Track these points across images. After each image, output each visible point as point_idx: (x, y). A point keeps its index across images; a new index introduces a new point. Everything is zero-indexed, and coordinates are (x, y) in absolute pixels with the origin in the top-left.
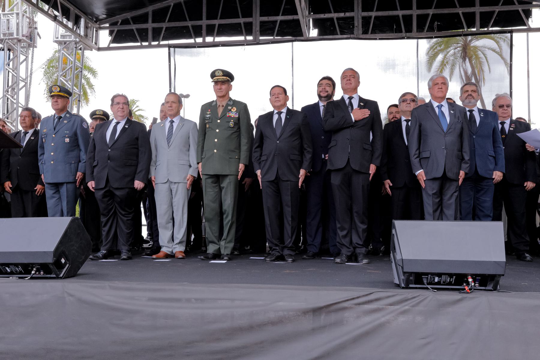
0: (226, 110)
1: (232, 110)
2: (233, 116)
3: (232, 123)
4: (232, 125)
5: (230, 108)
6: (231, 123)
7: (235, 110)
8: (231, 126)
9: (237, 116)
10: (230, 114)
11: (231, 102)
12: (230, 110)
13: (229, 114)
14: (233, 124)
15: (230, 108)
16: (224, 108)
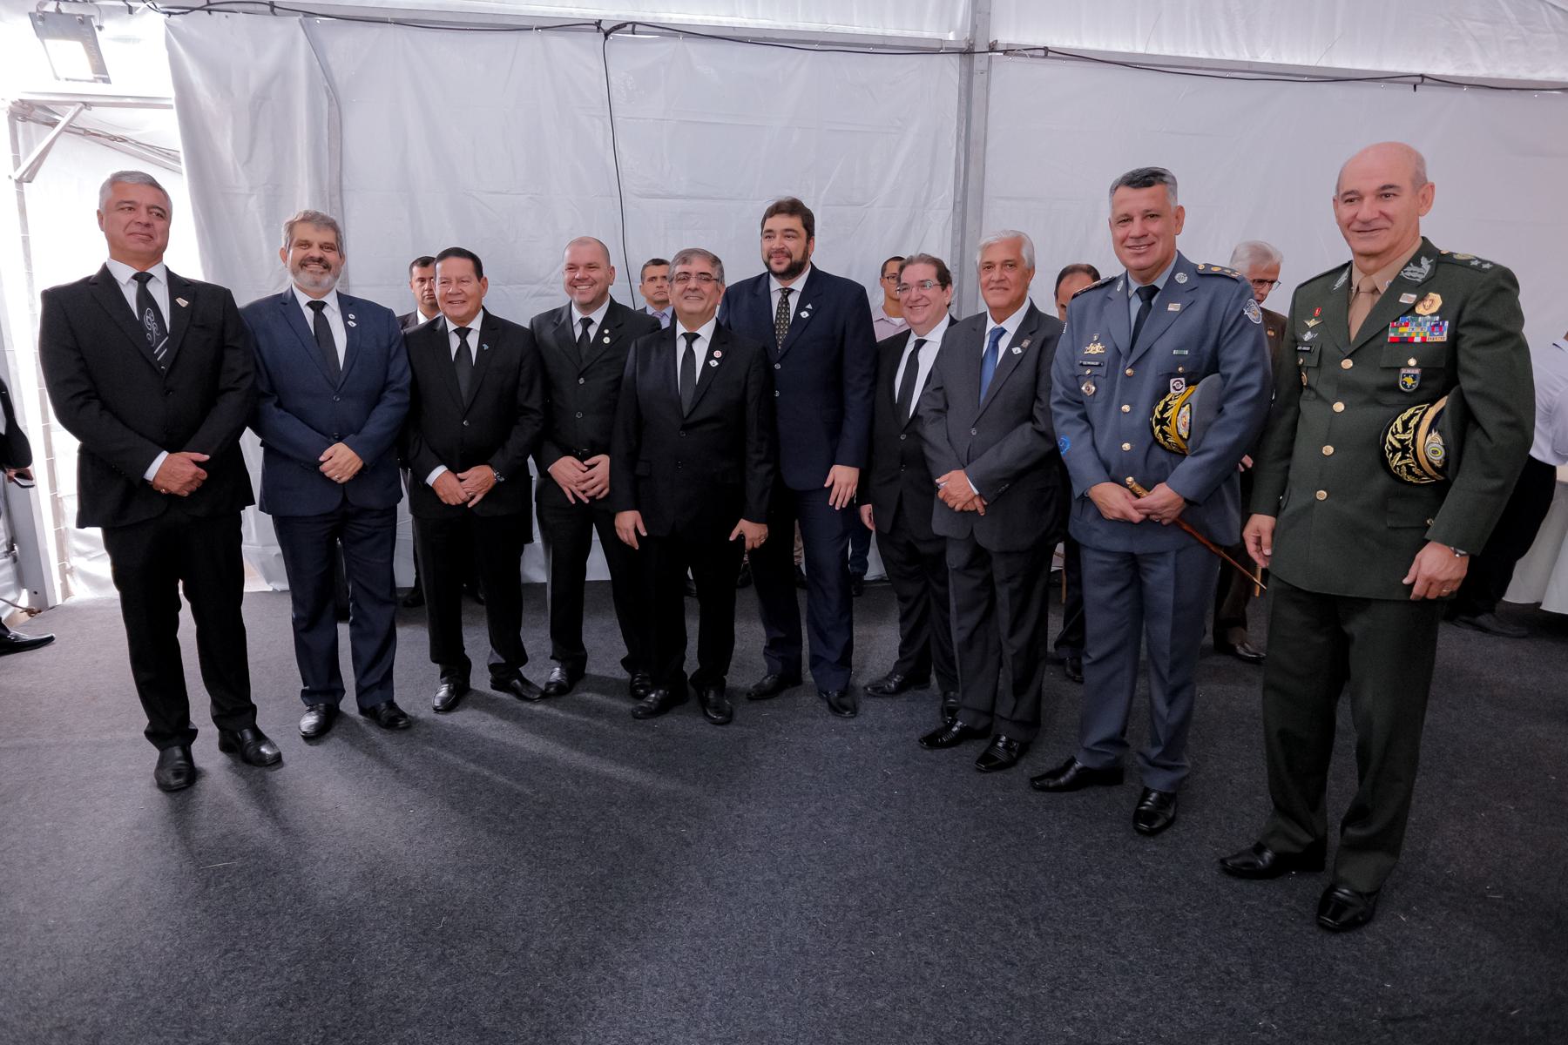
0: (1390, 308)
1: (1419, 310)
2: (1418, 340)
3: (1409, 371)
4: (1409, 381)
5: (1408, 298)
6: (1408, 375)
7: (1435, 309)
8: (1405, 386)
9: (1444, 337)
10: (1405, 331)
11: (1419, 265)
12: (1411, 310)
13: (1402, 330)
14: (1414, 379)
15: (1408, 298)
16: (1377, 298)
